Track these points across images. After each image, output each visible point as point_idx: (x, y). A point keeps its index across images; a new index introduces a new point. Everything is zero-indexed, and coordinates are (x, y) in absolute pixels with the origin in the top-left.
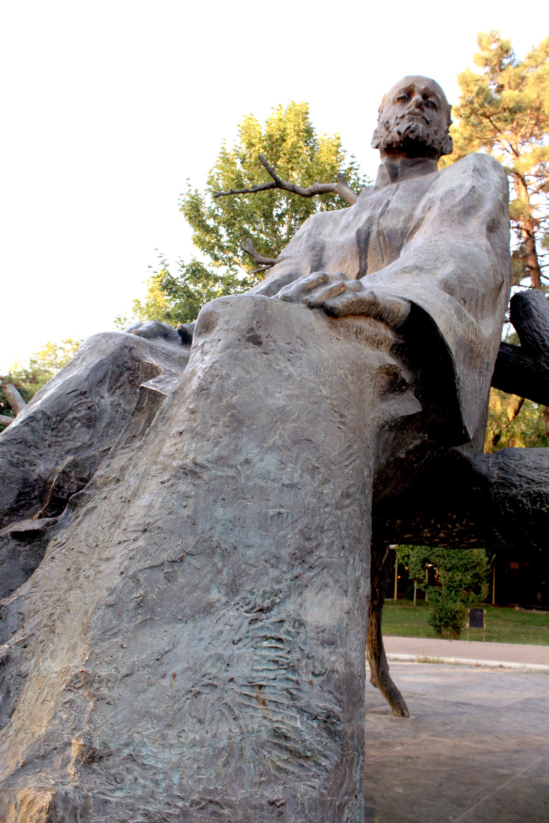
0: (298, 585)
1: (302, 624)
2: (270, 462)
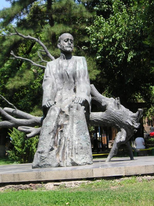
1: (87, 135)
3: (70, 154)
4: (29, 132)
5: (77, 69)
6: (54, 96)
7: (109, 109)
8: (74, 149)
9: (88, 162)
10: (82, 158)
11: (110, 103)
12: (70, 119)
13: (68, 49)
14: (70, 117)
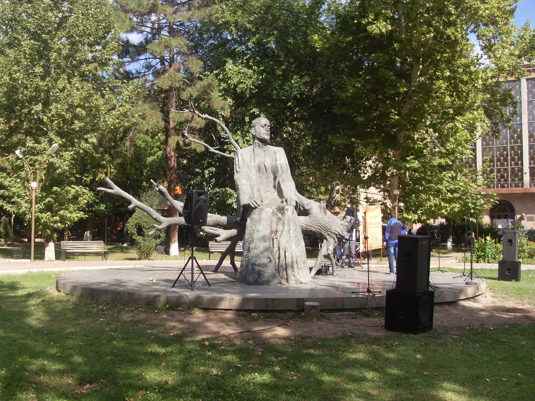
4: (218, 236)
5: (278, 163)
11: (314, 207)
14: (286, 221)
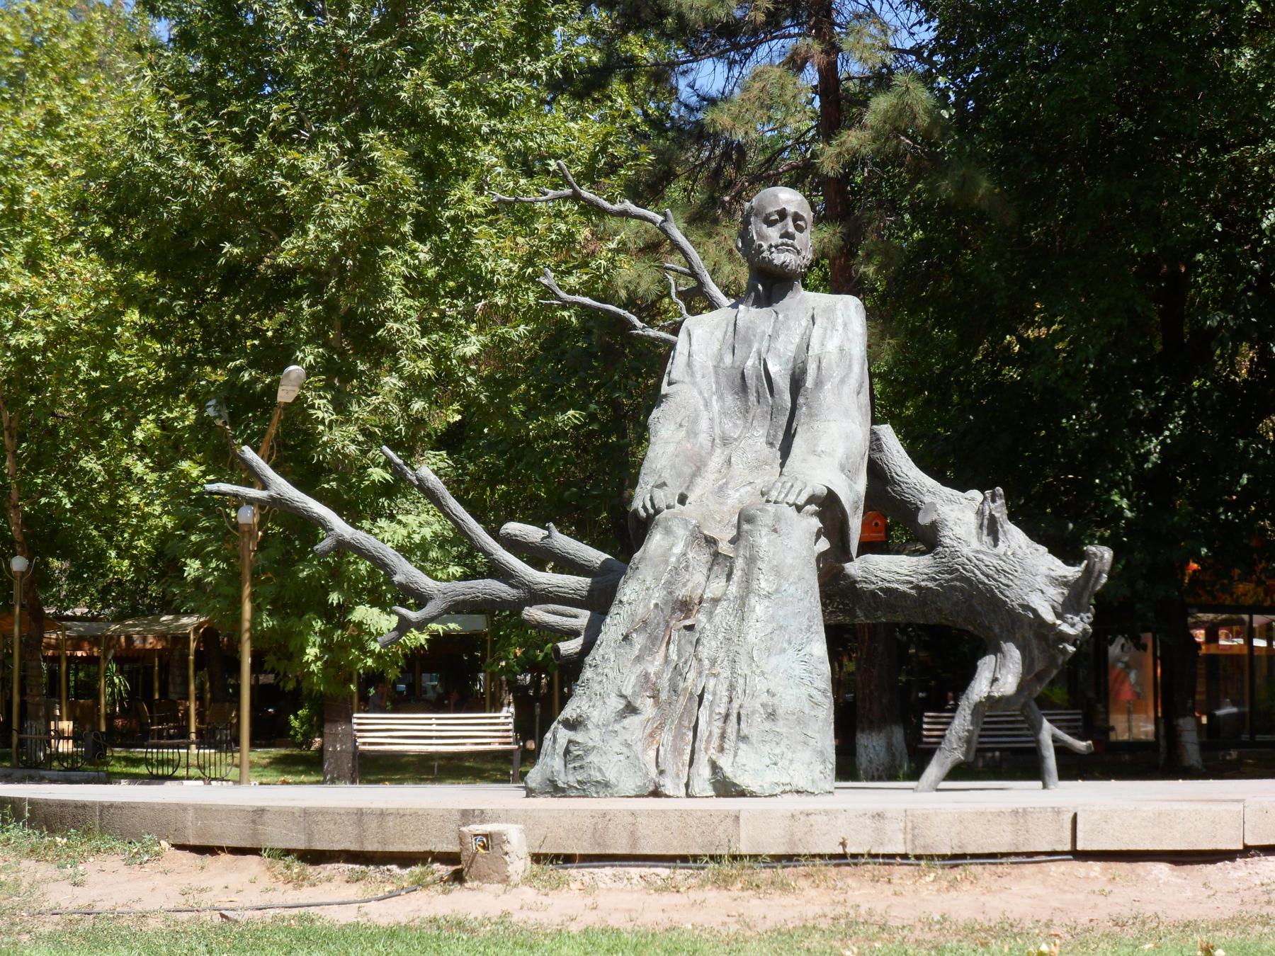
0: (810, 641)
2: (792, 590)
3: (715, 742)
5: (815, 349)
6: (688, 471)
7: (947, 541)
8: (733, 718)
9: (801, 784)
10: (768, 762)
12: (737, 574)
13: (779, 258)
14: (740, 563)
